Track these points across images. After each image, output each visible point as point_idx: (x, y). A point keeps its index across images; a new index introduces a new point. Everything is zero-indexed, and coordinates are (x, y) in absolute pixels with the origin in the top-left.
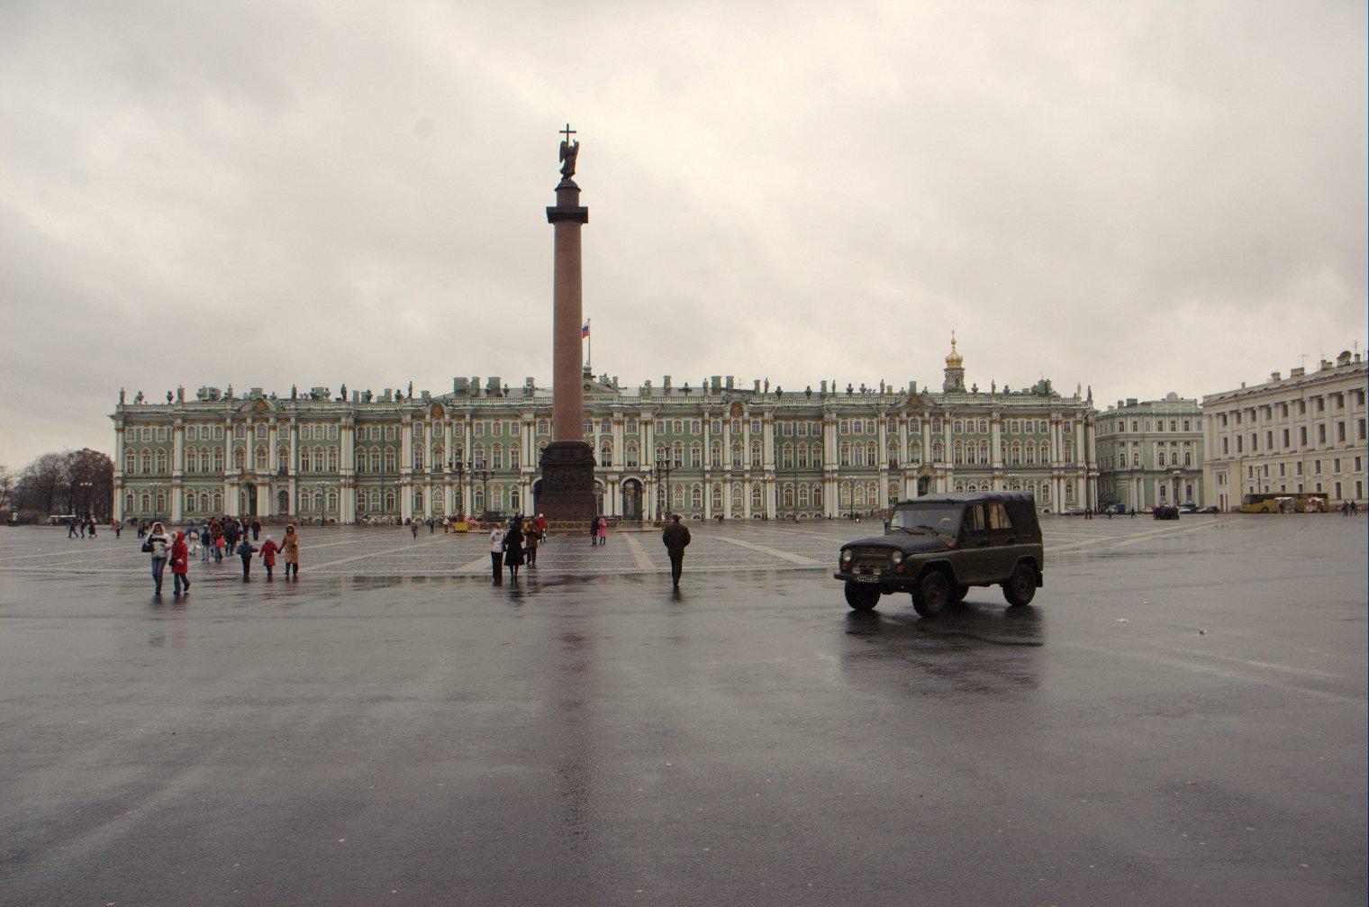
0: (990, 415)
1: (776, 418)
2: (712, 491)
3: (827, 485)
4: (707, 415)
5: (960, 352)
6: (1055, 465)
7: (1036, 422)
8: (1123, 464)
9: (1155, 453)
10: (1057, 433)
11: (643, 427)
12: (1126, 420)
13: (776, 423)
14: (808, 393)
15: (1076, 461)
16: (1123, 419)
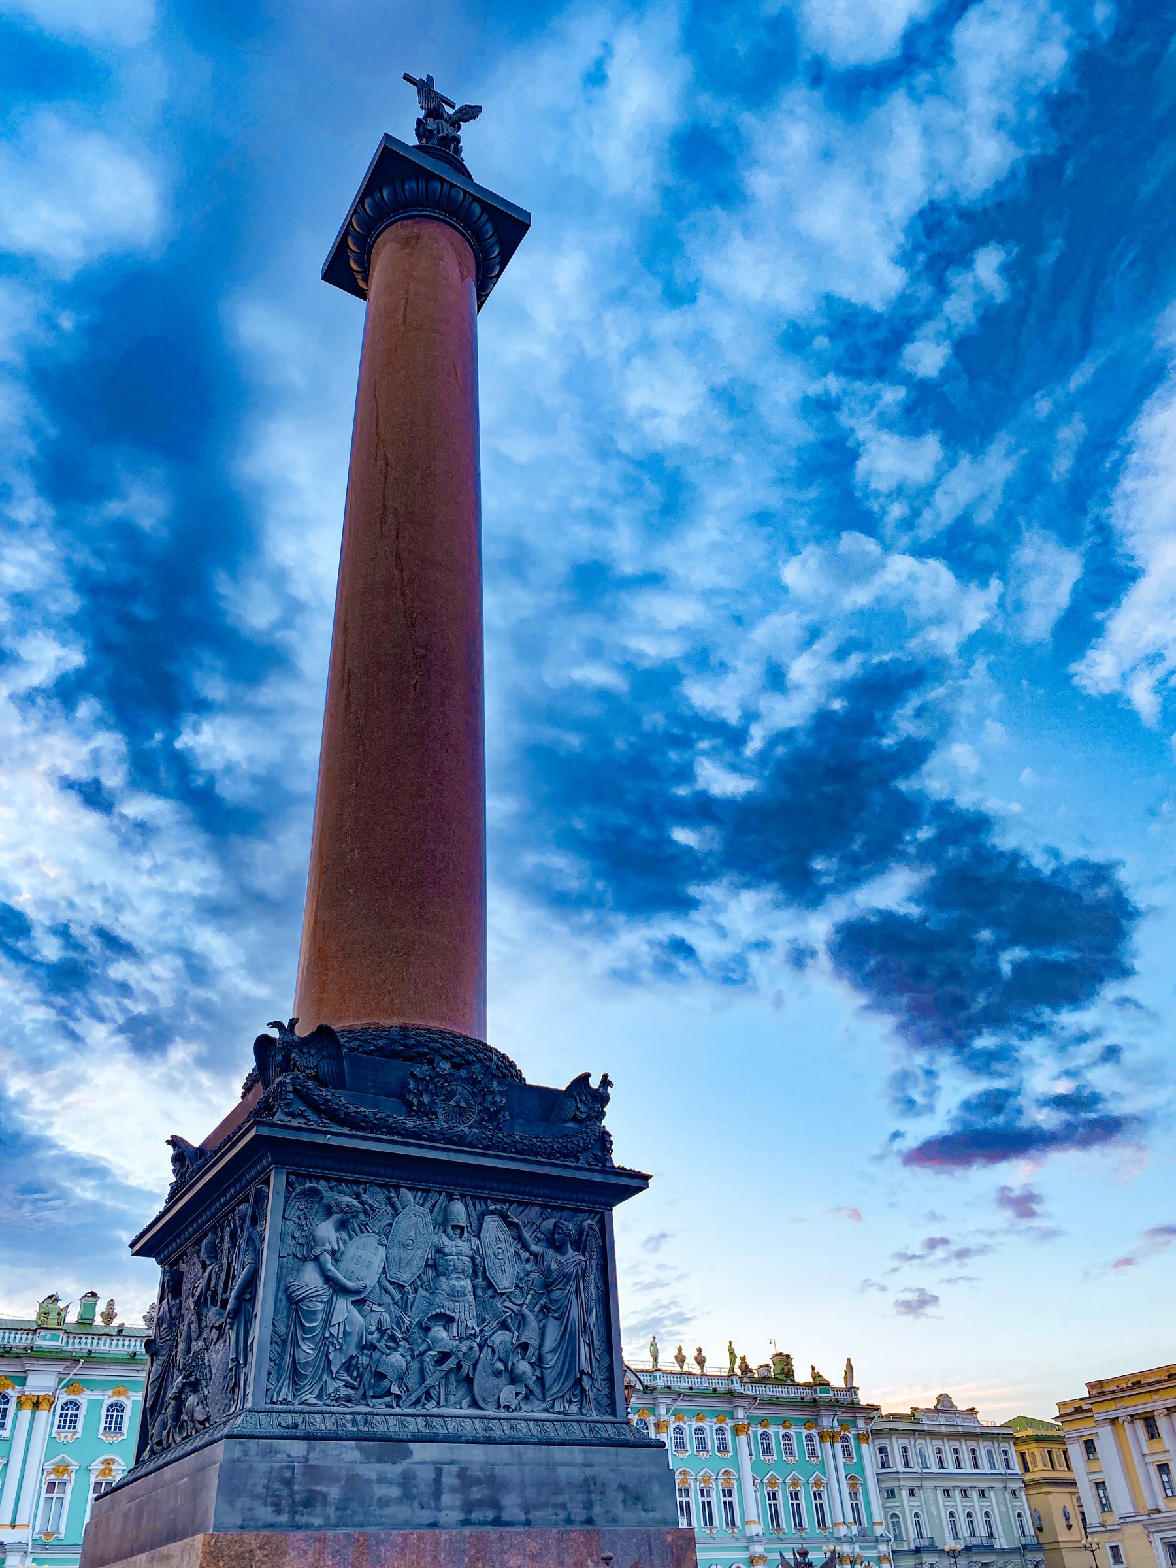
6: (843, 1531)
11: (26, 1413)
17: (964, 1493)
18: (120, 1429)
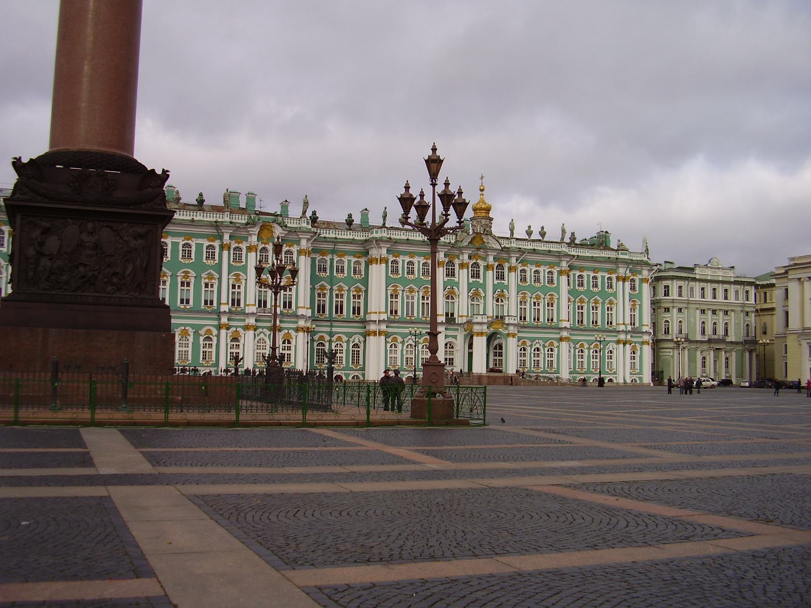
0: (558, 265)
1: (315, 251)
2: (229, 341)
3: (372, 337)
4: (226, 237)
6: (622, 328)
7: (603, 277)
8: (667, 332)
9: (698, 319)
10: (622, 290)
12: (672, 284)
13: (313, 256)
14: (350, 222)
15: (641, 325)
17: (714, 312)
18: (190, 256)
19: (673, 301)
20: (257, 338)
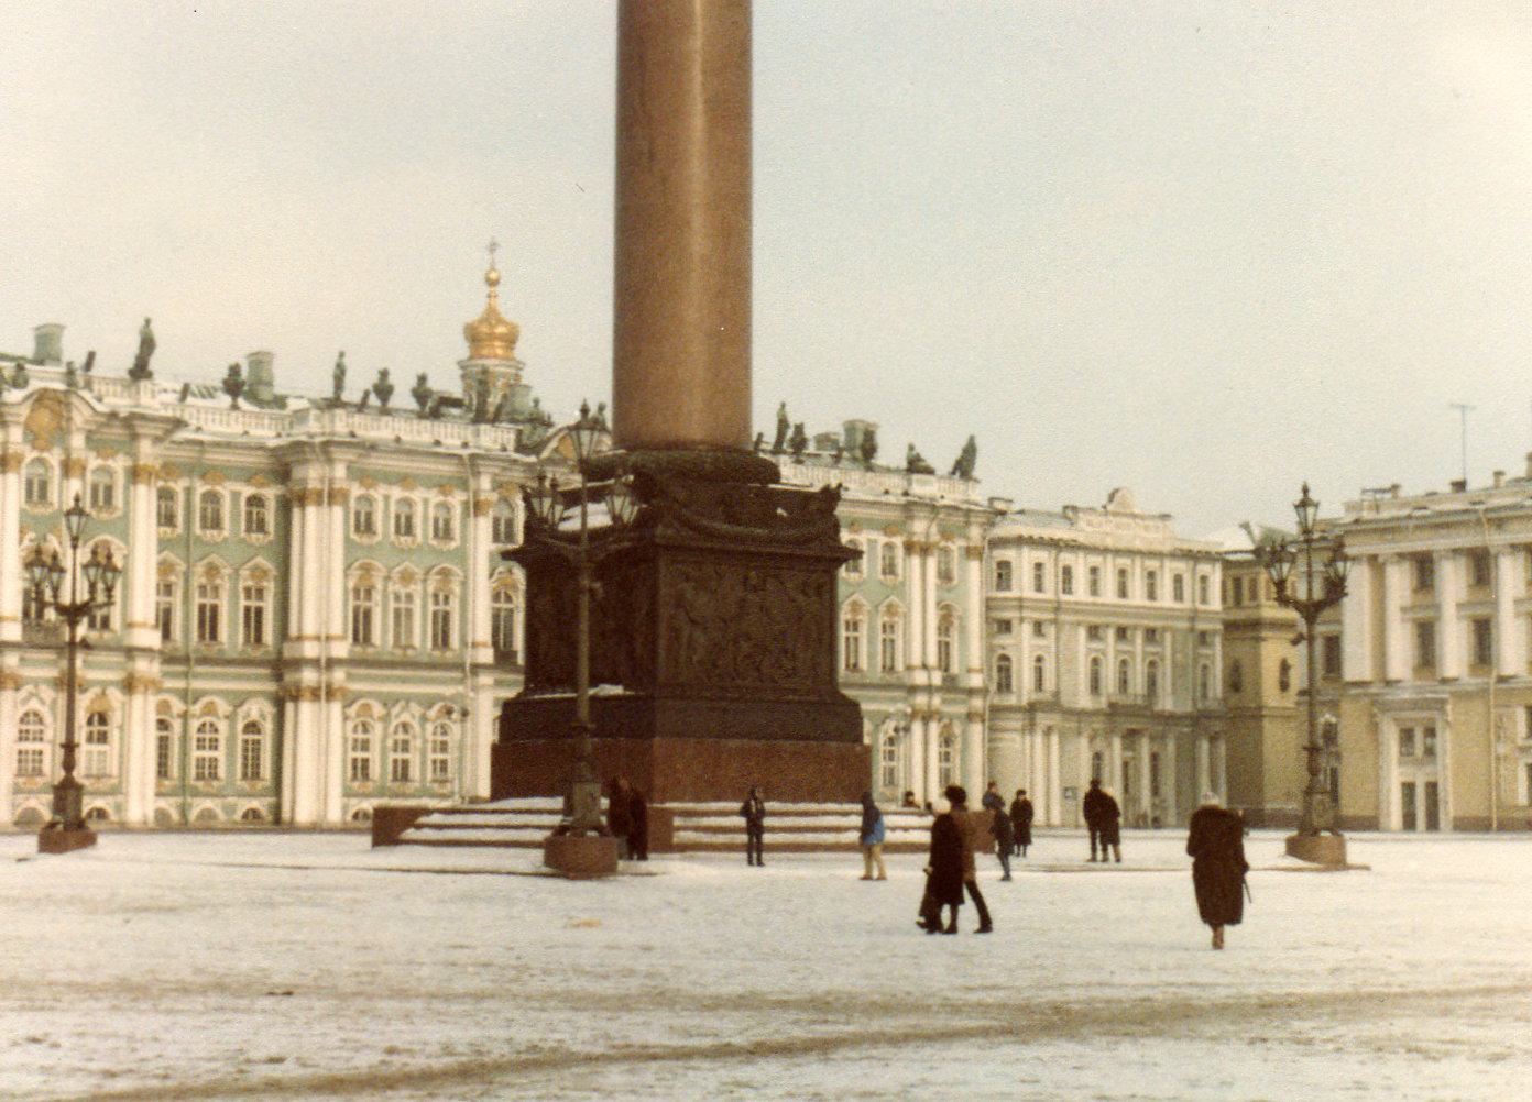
3: (307, 708)
5: (508, 308)
6: (920, 678)
16: (1008, 554)
17: (1122, 633)
19: (1020, 604)
20: (21, 711)
